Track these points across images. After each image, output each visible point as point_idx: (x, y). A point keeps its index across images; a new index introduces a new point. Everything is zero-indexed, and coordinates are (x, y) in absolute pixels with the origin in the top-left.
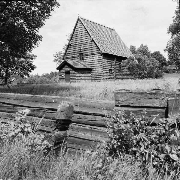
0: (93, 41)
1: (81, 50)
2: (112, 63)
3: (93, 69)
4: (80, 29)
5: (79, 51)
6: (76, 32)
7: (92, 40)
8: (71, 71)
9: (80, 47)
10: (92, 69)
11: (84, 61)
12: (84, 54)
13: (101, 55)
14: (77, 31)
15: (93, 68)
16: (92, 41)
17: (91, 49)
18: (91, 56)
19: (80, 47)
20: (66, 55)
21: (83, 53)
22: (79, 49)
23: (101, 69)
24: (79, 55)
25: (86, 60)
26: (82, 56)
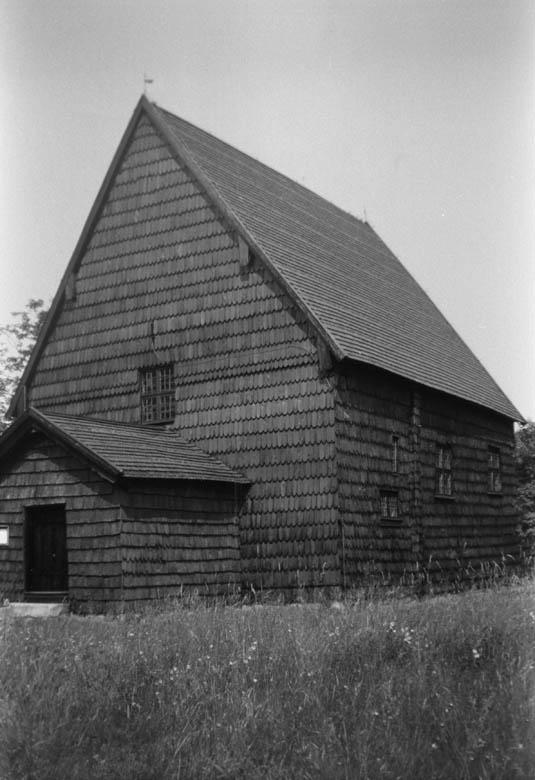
0: (254, 262)
1: (159, 342)
2: (396, 439)
3: (256, 490)
4: (145, 186)
5: (145, 344)
6: (117, 206)
7: (245, 258)
8: (78, 504)
9: (149, 313)
10: (248, 487)
11: (178, 421)
12: (180, 370)
13: (324, 375)
14: (131, 203)
15: (252, 475)
16: (244, 273)
17: (235, 328)
18: (241, 382)
19: (149, 313)
20: (38, 378)
21: (169, 367)
22: (144, 329)
23: (324, 484)
24: (133, 377)
25: (194, 419)
26: (159, 383)
